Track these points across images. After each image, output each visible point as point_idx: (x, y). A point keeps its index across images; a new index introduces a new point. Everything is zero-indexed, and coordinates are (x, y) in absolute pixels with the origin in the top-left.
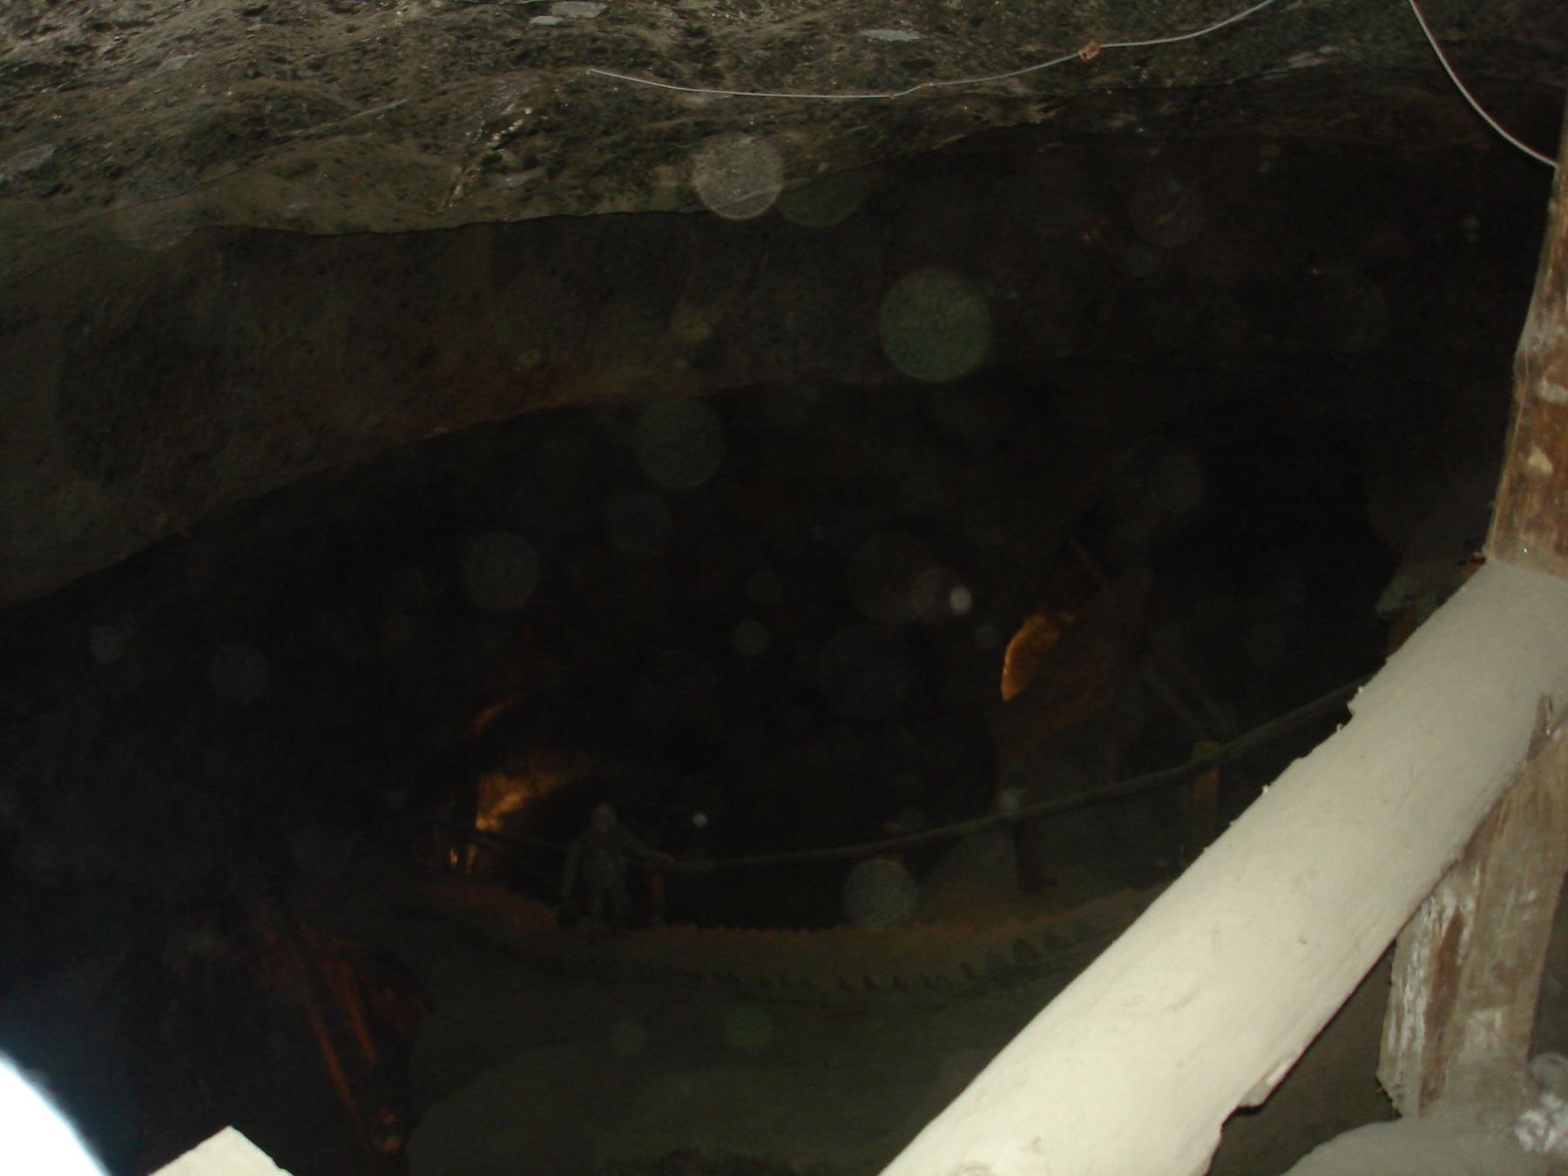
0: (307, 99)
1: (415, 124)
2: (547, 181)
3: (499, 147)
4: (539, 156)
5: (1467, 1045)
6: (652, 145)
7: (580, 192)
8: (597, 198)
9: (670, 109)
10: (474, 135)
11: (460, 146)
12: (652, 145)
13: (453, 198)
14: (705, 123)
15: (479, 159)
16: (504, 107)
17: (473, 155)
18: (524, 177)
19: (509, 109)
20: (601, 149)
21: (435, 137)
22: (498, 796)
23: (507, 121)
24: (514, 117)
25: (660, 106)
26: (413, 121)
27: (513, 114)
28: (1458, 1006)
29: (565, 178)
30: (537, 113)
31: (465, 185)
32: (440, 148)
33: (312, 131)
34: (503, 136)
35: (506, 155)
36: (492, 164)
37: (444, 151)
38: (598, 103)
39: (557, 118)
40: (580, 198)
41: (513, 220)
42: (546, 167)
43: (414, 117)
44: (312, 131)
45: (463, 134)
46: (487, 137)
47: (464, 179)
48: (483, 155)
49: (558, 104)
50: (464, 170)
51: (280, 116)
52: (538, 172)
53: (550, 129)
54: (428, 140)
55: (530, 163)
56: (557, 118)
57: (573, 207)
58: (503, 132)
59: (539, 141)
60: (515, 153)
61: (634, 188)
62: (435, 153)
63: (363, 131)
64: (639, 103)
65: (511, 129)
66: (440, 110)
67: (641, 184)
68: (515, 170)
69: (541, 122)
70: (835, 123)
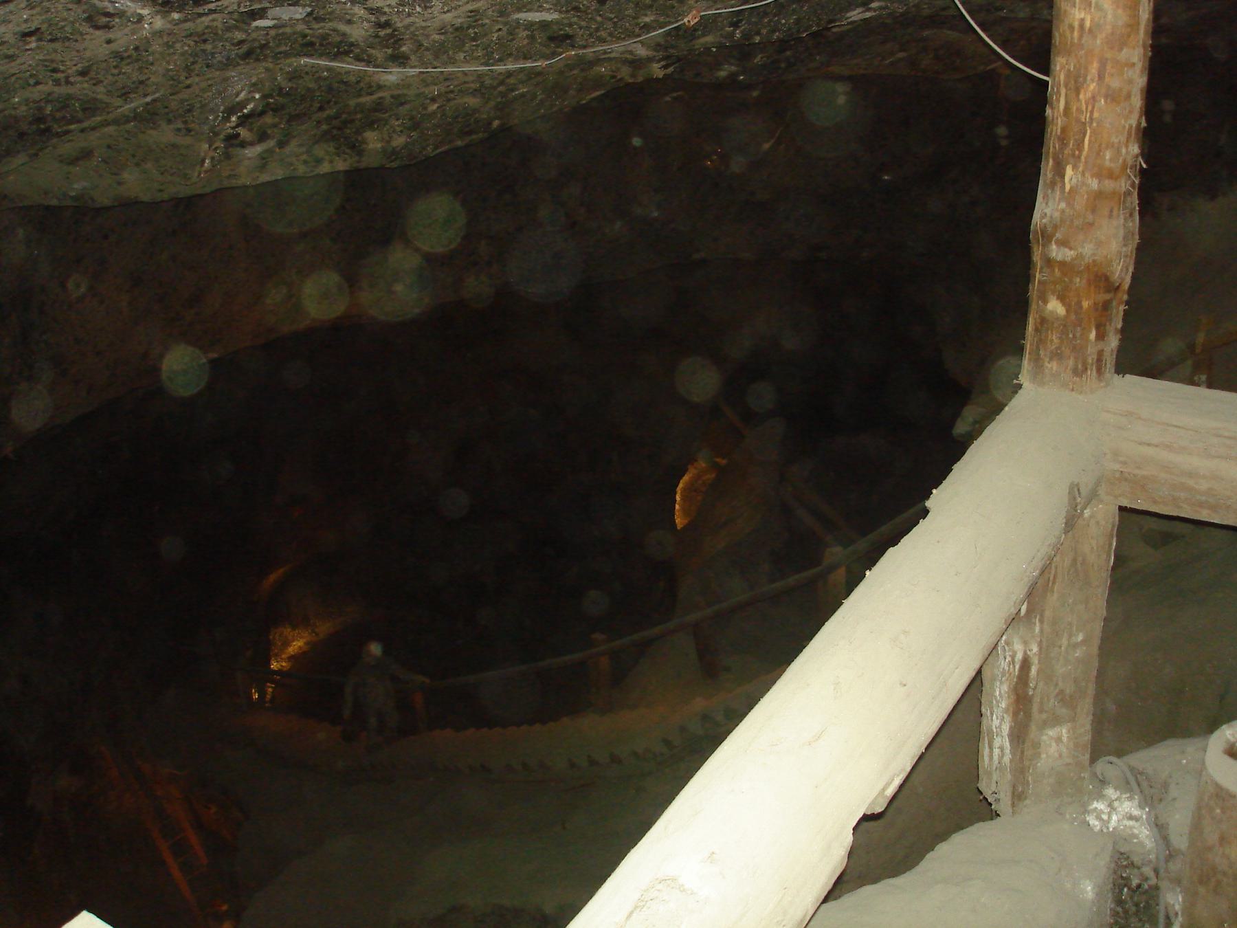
0: (79, 99)
1: (167, 114)
2: (277, 150)
3: (237, 126)
5: (1044, 756)
6: (359, 116)
7: (304, 157)
8: (319, 161)
9: (370, 87)
10: (215, 120)
12: (359, 116)
13: (204, 169)
14: (399, 96)
15: (222, 137)
16: (237, 95)
17: (216, 134)
18: (259, 149)
19: (242, 95)
20: (319, 122)
21: (185, 122)
22: (286, 644)
23: (243, 105)
26: (166, 110)
27: (246, 99)
28: (1033, 727)
29: (293, 146)
30: (264, 97)
31: (213, 158)
32: (189, 130)
33: (86, 124)
34: (239, 118)
35: (243, 133)
36: (232, 140)
37: (193, 133)
38: (312, 85)
39: (281, 100)
40: (305, 162)
41: (254, 184)
42: (275, 140)
43: (167, 107)
44: (86, 124)
45: (208, 118)
46: (227, 119)
48: (224, 134)
49: (281, 89)
50: (210, 146)
52: (271, 143)
53: (276, 110)
54: (180, 125)
55: (263, 137)
56: (281, 100)
57: (302, 170)
58: (239, 114)
59: (268, 119)
60: (251, 130)
61: (348, 151)
62: (186, 135)
63: (128, 121)
64: (345, 83)
66: (187, 101)
67: (353, 147)
68: (252, 144)
69: (268, 104)
70: (502, 88)
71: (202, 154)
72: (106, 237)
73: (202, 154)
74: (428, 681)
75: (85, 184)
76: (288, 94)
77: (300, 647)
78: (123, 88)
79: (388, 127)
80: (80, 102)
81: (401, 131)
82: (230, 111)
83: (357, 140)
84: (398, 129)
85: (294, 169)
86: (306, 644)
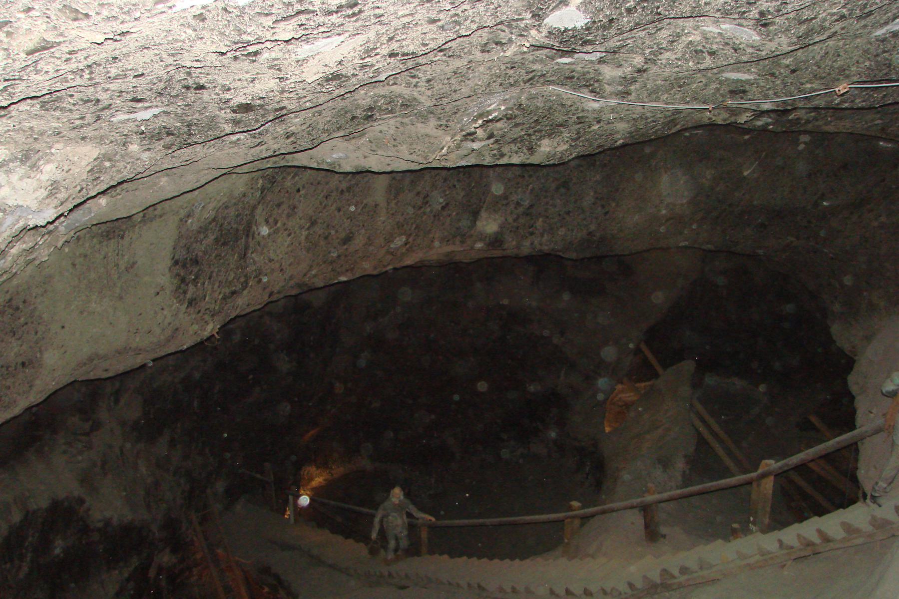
4: (495, 133)
7: (495, 152)
8: (502, 155)
10: (466, 121)
11: (459, 126)
13: (440, 154)
21: (447, 121)
22: (311, 479)
23: (489, 113)
24: (495, 110)
25: (573, 108)
30: (507, 109)
31: (449, 147)
35: (480, 133)
37: (448, 128)
39: (516, 112)
46: (474, 121)
47: (450, 144)
50: (451, 139)
51: (385, 107)
53: (509, 118)
55: (491, 136)
56: (516, 112)
58: (485, 119)
60: (485, 131)
64: (563, 105)
65: (490, 117)
68: (480, 140)
71: (444, 143)
72: (298, 191)
73: (444, 143)
74: (433, 519)
75: (341, 155)
76: (523, 109)
77: (320, 482)
78: (443, 94)
79: (561, 137)
80: (403, 100)
81: (567, 141)
82: (480, 116)
83: (536, 144)
84: (566, 139)
85: (484, 159)
86: (325, 480)
